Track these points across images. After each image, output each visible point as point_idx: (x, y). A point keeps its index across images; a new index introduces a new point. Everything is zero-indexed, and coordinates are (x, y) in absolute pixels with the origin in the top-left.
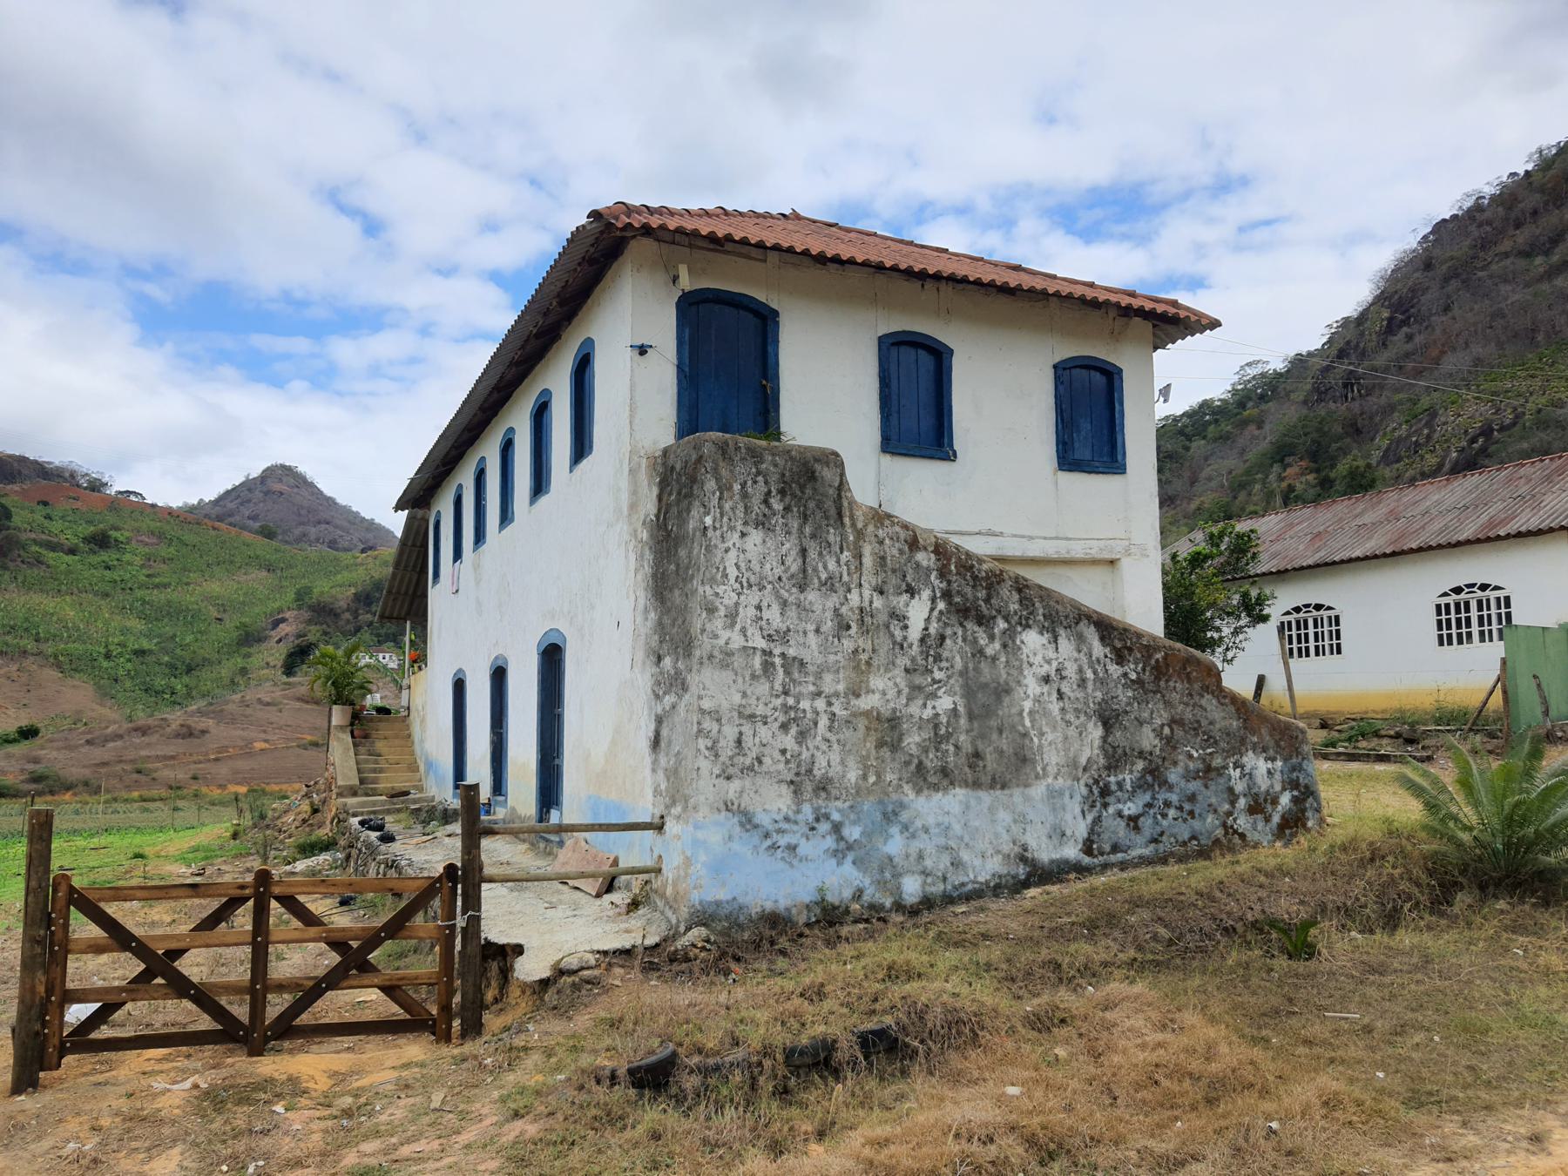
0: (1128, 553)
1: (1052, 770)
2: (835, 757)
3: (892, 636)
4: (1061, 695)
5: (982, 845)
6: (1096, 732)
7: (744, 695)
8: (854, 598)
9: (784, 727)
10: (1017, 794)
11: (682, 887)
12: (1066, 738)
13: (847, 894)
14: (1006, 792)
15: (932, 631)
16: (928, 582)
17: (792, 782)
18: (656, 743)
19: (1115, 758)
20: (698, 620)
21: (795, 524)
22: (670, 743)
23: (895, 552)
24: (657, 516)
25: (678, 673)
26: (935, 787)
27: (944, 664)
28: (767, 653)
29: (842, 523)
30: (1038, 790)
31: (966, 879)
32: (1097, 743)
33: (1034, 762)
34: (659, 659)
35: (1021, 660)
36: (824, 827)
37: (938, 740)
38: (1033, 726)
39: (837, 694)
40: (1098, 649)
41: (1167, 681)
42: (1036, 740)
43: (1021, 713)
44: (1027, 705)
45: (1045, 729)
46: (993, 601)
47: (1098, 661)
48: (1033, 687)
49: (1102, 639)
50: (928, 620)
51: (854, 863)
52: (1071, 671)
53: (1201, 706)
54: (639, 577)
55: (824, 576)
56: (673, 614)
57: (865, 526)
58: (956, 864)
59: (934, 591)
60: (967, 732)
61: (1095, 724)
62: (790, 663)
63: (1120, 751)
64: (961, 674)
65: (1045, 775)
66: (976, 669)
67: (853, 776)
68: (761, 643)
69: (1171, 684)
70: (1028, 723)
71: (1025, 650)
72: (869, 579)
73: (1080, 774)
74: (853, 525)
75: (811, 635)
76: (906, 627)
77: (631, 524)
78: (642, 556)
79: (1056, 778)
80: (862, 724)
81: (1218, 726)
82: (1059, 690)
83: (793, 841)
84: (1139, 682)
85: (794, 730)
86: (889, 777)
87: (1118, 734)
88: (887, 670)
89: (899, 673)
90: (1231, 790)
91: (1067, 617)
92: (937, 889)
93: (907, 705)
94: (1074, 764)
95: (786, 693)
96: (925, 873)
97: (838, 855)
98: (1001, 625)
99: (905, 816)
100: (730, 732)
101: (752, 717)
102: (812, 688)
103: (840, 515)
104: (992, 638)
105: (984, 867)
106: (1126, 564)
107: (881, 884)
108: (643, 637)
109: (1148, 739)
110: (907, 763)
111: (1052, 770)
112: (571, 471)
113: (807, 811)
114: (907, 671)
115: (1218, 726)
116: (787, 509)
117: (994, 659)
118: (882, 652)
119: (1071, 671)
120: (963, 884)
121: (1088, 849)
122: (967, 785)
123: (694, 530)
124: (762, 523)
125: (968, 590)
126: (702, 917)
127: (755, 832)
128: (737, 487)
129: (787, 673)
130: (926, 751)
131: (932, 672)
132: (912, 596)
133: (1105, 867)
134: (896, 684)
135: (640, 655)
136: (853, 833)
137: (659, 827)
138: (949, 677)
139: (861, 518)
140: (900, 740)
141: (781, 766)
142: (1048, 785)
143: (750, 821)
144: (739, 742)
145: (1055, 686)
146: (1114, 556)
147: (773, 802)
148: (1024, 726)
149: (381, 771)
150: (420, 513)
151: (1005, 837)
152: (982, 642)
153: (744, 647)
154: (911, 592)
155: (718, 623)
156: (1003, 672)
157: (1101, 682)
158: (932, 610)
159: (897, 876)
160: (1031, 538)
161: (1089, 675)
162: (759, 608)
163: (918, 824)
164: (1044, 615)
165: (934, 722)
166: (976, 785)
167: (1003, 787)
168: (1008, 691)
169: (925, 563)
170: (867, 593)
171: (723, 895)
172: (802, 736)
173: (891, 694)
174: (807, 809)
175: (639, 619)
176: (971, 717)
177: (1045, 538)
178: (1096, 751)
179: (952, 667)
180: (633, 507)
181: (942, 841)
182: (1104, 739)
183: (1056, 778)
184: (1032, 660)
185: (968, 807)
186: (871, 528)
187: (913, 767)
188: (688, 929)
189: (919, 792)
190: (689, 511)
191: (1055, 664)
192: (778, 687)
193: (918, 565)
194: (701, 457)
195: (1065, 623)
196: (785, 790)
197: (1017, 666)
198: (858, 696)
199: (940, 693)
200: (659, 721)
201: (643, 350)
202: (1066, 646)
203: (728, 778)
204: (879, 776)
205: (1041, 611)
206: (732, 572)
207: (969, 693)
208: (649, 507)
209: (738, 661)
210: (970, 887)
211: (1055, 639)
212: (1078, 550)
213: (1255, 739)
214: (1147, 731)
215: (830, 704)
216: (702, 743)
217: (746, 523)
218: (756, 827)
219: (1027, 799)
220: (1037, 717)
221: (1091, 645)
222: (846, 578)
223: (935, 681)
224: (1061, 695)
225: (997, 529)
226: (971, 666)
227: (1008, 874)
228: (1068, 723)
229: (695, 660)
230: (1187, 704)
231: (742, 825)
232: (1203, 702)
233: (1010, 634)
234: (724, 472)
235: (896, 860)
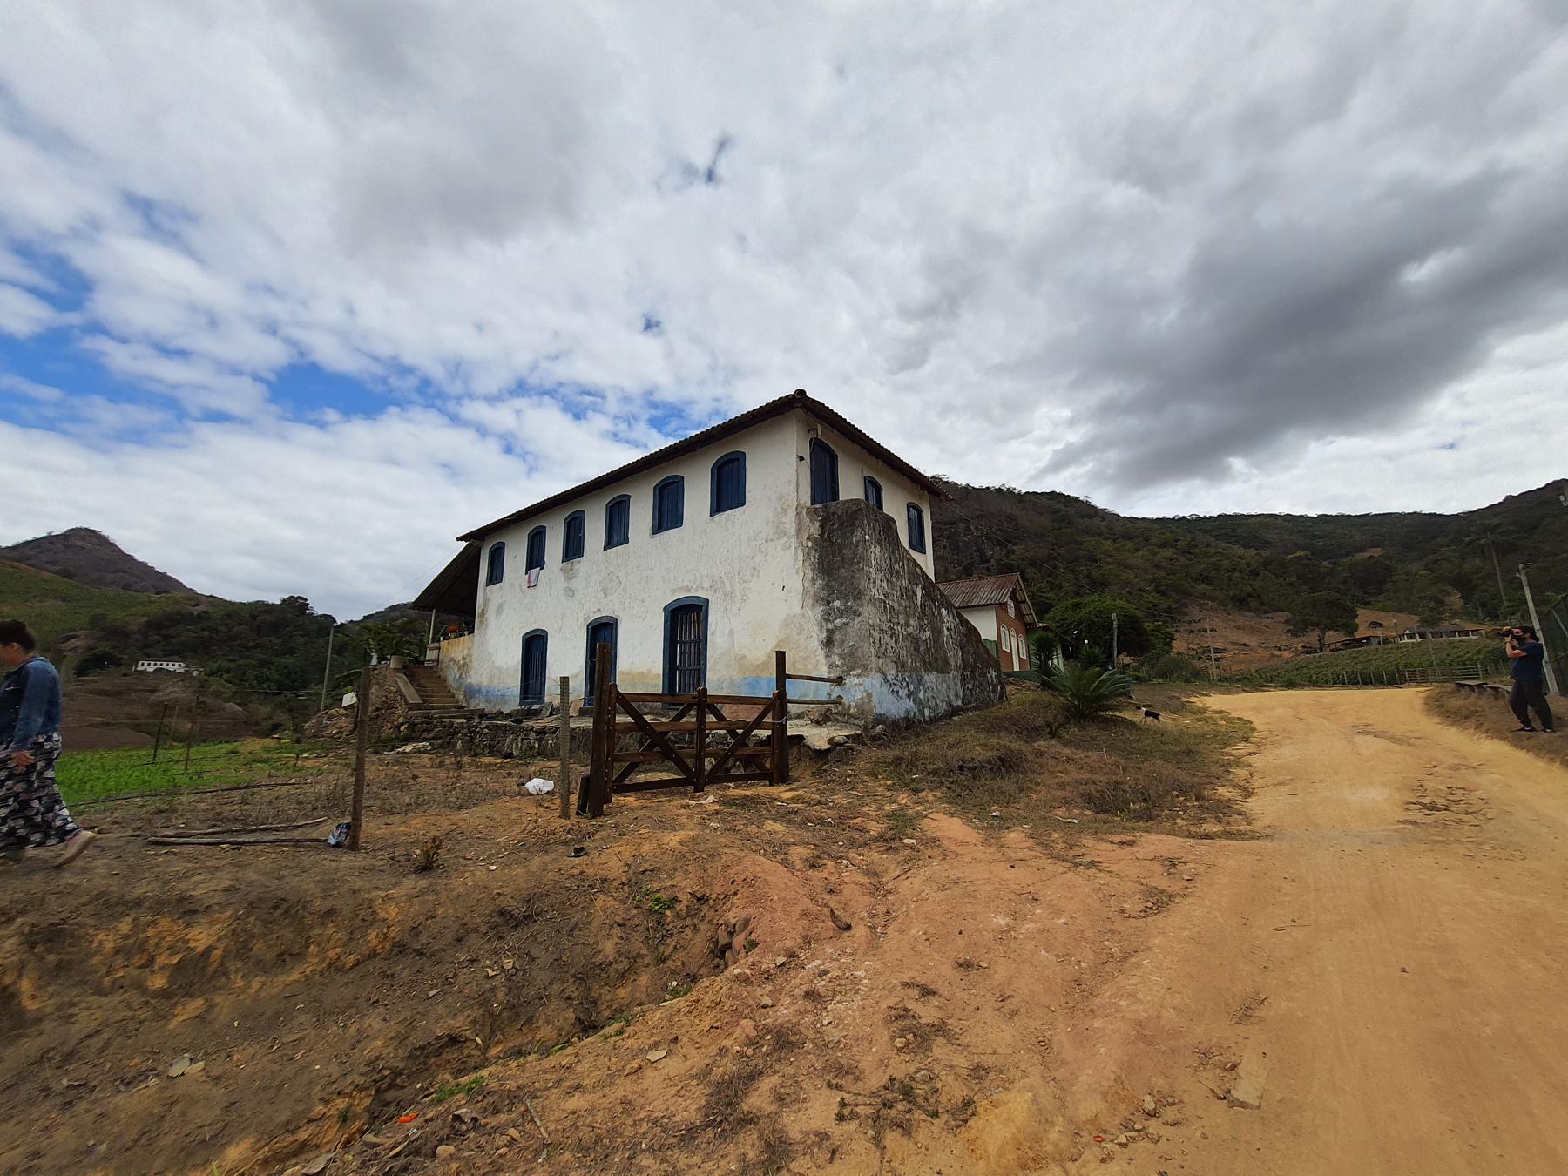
5: (941, 698)
11: (867, 708)
18: (828, 643)
19: (965, 664)
20: (864, 583)
21: (888, 546)
22: (843, 641)
24: (822, 535)
25: (847, 609)
34: (828, 602)
36: (905, 684)
40: (958, 620)
52: (952, 627)
54: (807, 564)
56: (841, 580)
58: (936, 704)
62: (892, 608)
67: (909, 662)
68: (883, 598)
77: (798, 538)
78: (808, 554)
86: (918, 664)
90: (988, 682)
96: (930, 708)
97: (909, 696)
99: (923, 681)
101: (883, 630)
108: (812, 593)
109: (971, 660)
112: (711, 516)
119: (952, 627)
121: (963, 702)
122: (937, 671)
123: (858, 542)
126: (879, 719)
133: (967, 709)
135: (810, 602)
136: (911, 687)
137: (839, 681)
147: (891, 673)
149: (431, 696)
150: (477, 542)
159: (923, 708)
168: (941, 632)
172: (896, 642)
175: (806, 584)
180: (799, 531)
181: (931, 694)
188: (874, 727)
190: (852, 533)
194: (861, 509)
197: (942, 622)
200: (830, 632)
201: (801, 459)
208: (814, 530)
216: (872, 640)
218: (888, 681)
219: (949, 679)
229: (865, 602)
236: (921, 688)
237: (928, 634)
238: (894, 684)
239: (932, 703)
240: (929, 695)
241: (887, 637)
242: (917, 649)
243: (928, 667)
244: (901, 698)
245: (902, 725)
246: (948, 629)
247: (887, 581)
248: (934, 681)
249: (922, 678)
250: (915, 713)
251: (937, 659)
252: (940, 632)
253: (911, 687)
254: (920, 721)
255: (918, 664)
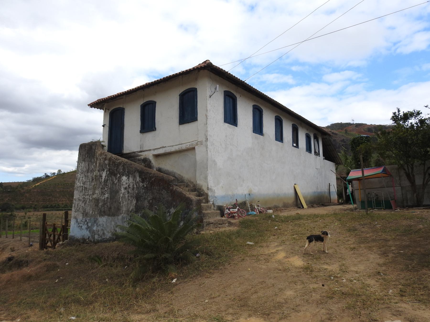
0: (197, 144)
1: (124, 212)
2: (89, 208)
3: (100, 181)
4: (128, 193)
6: (134, 202)
7: (79, 196)
8: (95, 173)
9: (83, 202)
10: (116, 217)
12: (128, 204)
13: (87, 237)
14: (114, 217)
15: (106, 179)
16: (106, 168)
17: (83, 213)
19: (138, 209)
23: (102, 161)
26: (102, 216)
27: (107, 186)
28: (82, 187)
29: (94, 157)
30: (120, 217)
31: (105, 238)
32: (134, 205)
33: (120, 210)
35: (121, 184)
36: (86, 223)
37: (104, 204)
38: (122, 201)
39: (91, 195)
40: (138, 179)
41: (154, 186)
42: (122, 204)
43: (120, 198)
44: (121, 195)
45: (124, 201)
46: (118, 170)
47: (138, 182)
48: (123, 191)
49: (140, 176)
50: (105, 176)
51: (89, 231)
52: (131, 186)
53: (162, 194)
55: (91, 169)
57: (98, 157)
58: (104, 234)
59: (107, 169)
60: (110, 202)
61: (135, 200)
63: (139, 207)
64: (110, 189)
65: (122, 213)
66: (113, 187)
67: (91, 212)
68: (82, 185)
69: (155, 187)
70: (121, 200)
71: (122, 181)
72: (97, 169)
73: (129, 213)
74: (96, 157)
75: (88, 182)
76: (102, 179)
79: (124, 214)
80: (93, 201)
81: (165, 200)
82: (128, 191)
83: (82, 225)
84: (147, 187)
85: (84, 203)
87: (139, 202)
88: (98, 189)
89: (100, 189)
91: (132, 171)
92: (100, 239)
93: (100, 197)
94: (128, 210)
95: (84, 195)
96: (99, 235)
97: (87, 229)
98: (119, 175)
100: (77, 203)
101: (80, 200)
102: (87, 194)
103: (94, 156)
104: (116, 179)
105: (108, 235)
106: (196, 147)
107: (92, 236)
110: (99, 210)
111: (124, 212)
113: (84, 220)
114: (101, 189)
115: (165, 200)
116: (87, 156)
117: (116, 184)
118: (98, 185)
119: (131, 186)
120: (104, 238)
124: (84, 160)
125: (113, 168)
127: (77, 223)
128: (82, 154)
129: (85, 191)
130: (102, 207)
131: (105, 188)
132: (103, 172)
134: (99, 192)
136: (90, 224)
138: (108, 189)
139: (98, 155)
140: (98, 204)
141: (82, 210)
142: (122, 216)
143: (77, 221)
144: (78, 205)
145: (127, 190)
146: (193, 146)
147: (80, 218)
148: (120, 201)
151: (113, 228)
152: (114, 180)
153: (80, 186)
154: (103, 170)
155: (77, 181)
156: (117, 187)
157: (137, 188)
158: (106, 174)
159: (95, 235)
160: (173, 146)
161: (135, 186)
162: (82, 178)
163: (99, 223)
164: (127, 172)
165: (104, 200)
166: (109, 215)
167: (114, 216)
169: (106, 163)
170: (97, 172)
171: (73, 235)
173: (99, 194)
174: (84, 219)
176: (111, 199)
177: (176, 145)
178: (134, 207)
179: (108, 187)
181: (102, 228)
182: (136, 204)
183: (124, 214)
184: (123, 184)
185: (107, 220)
186: (99, 157)
187: (100, 211)
189: (100, 216)
191: (128, 184)
192: (83, 194)
193: (105, 163)
195: (131, 173)
196: (82, 215)
197: (120, 185)
198: (93, 195)
199: (106, 193)
202: (131, 179)
203: (76, 212)
204: (95, 213)
205: (127, 171)
206: (80, 171)
207: (111, 193)
209: (79, 189)
210: (105, 239)
211: (129, 178)
212: (184, 147)
213: (175, 204)
214: (146, 202)
215: (89, 197)
217: (82, 161)
219: (118, 219)
220: (123, 198)
221: (137, 178)
222: (94, 169)
223: (105, 191)
224: (128, 192)
225: (164, 146)
226: (112, 186)
227: (112, 238)
228: (129, 200)
230: (158, 193)
231: (76, 221)
232: (162, 192)
233: (120, 177)
234: (81, 151)
235: (95, 231)
236: (95, 225)
237: (106, 196)
238: (80, 223)
239: (101, 233)
240: (100, 228)
241: (81, 203)
242: (97, 205)
243: (102, 214)
244: (83, 229)
245: (81, 241)
246: (126, 188)
247: (85, 176)
248: (105, 221)
249: (97, 219)
250: (89, 237)
251: (110, 208)
252: (117, 192)
253: (90, 224)
254: (91, 241)
255: (96, 213)
